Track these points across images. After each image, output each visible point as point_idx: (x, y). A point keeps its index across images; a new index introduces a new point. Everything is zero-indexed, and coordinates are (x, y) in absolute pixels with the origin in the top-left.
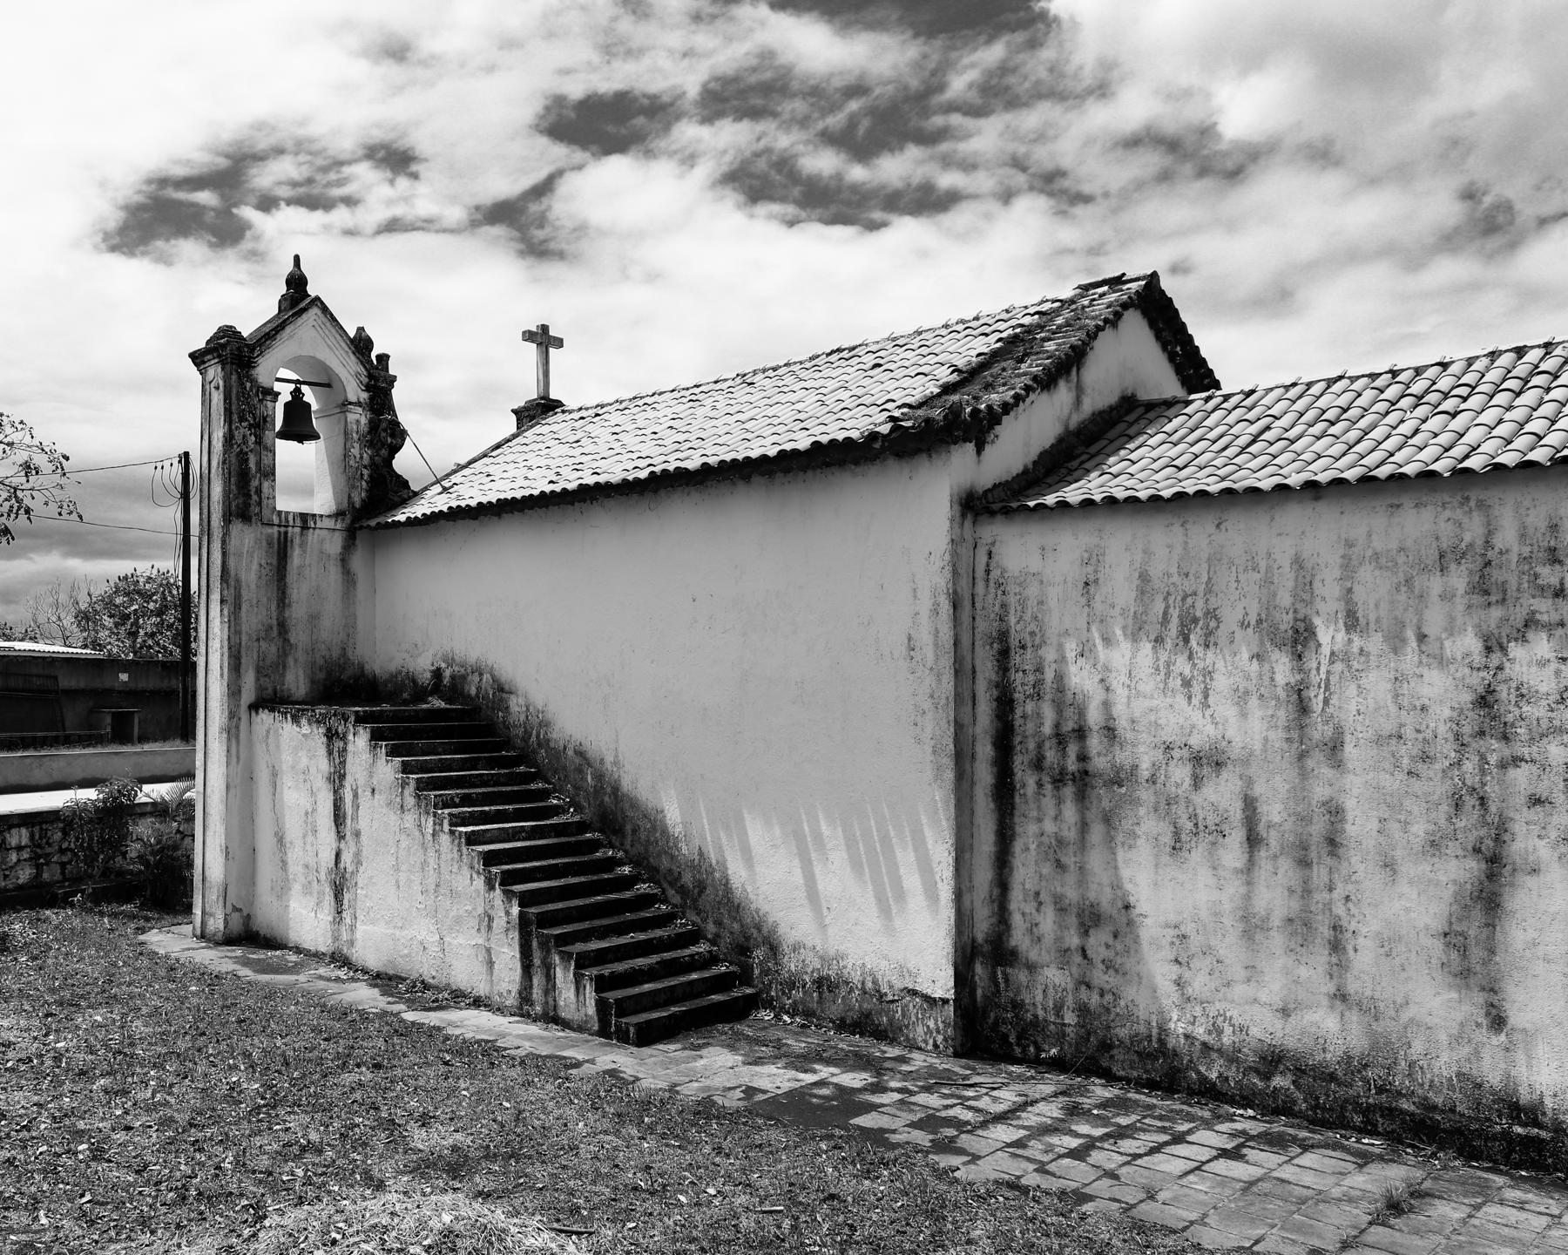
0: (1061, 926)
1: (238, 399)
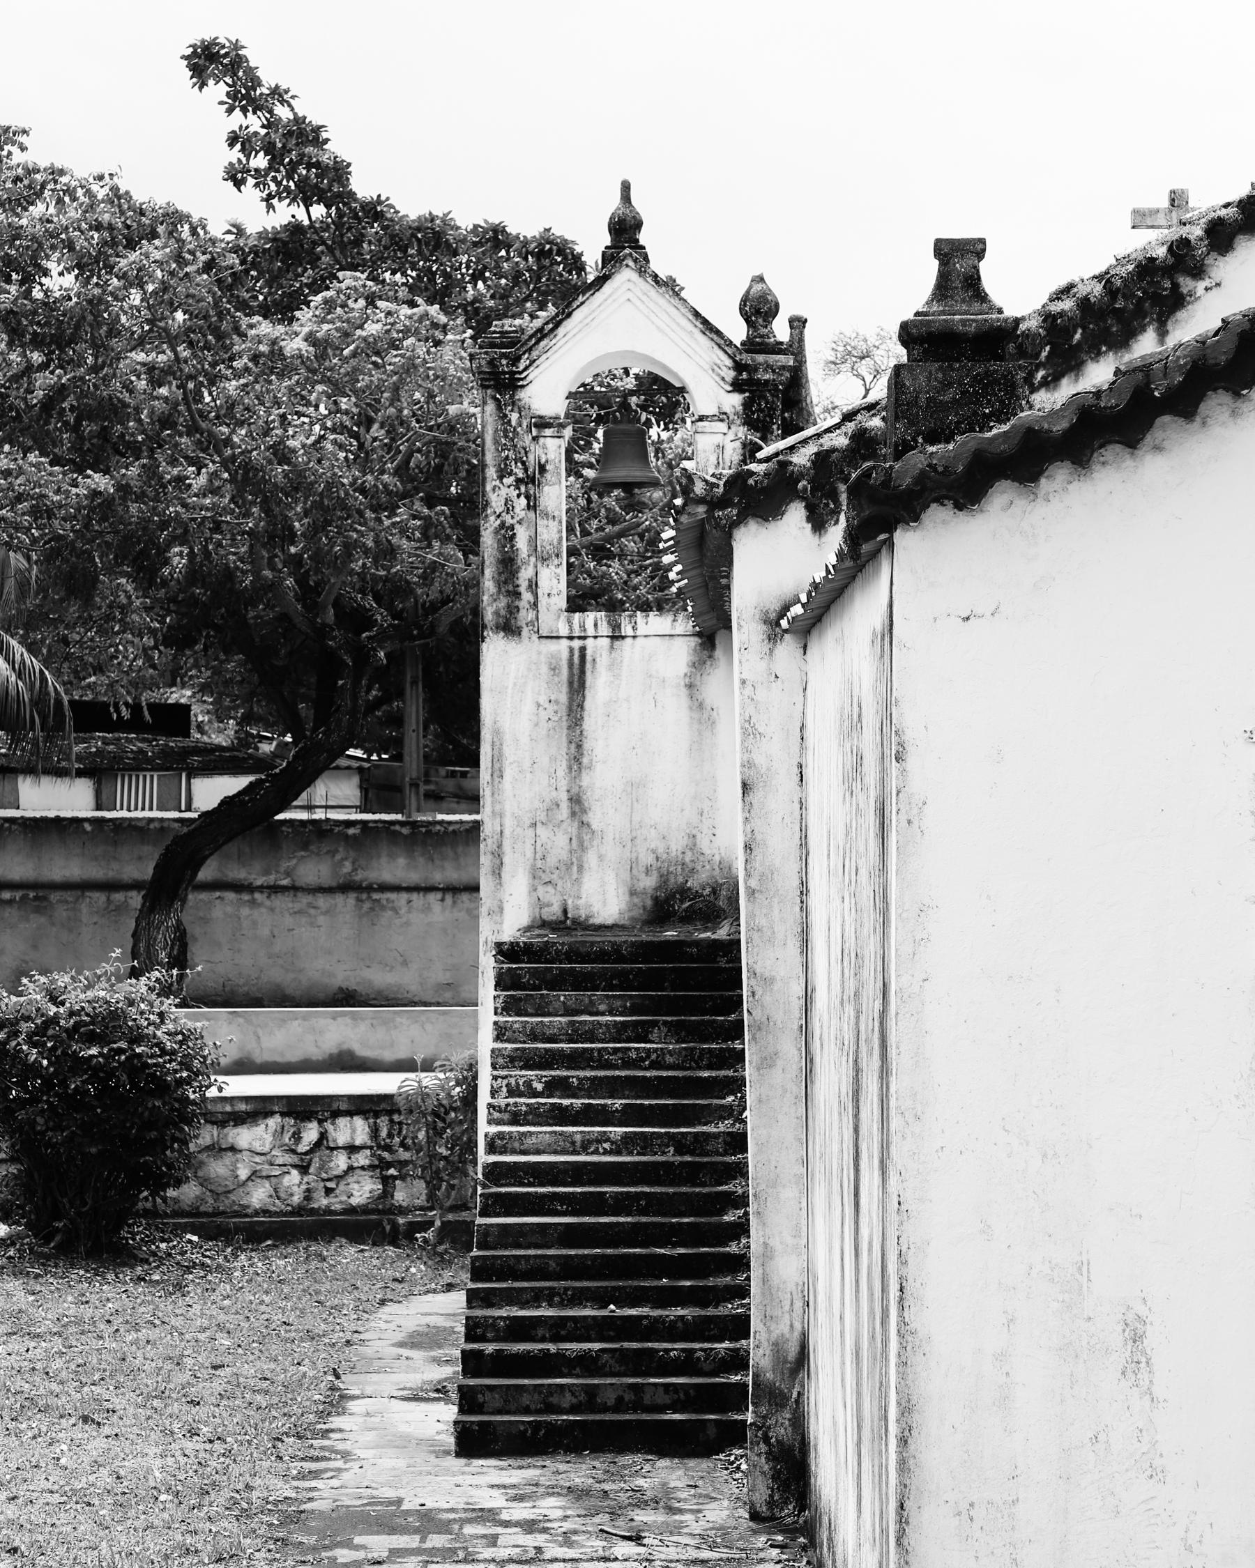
1: (496, 442)
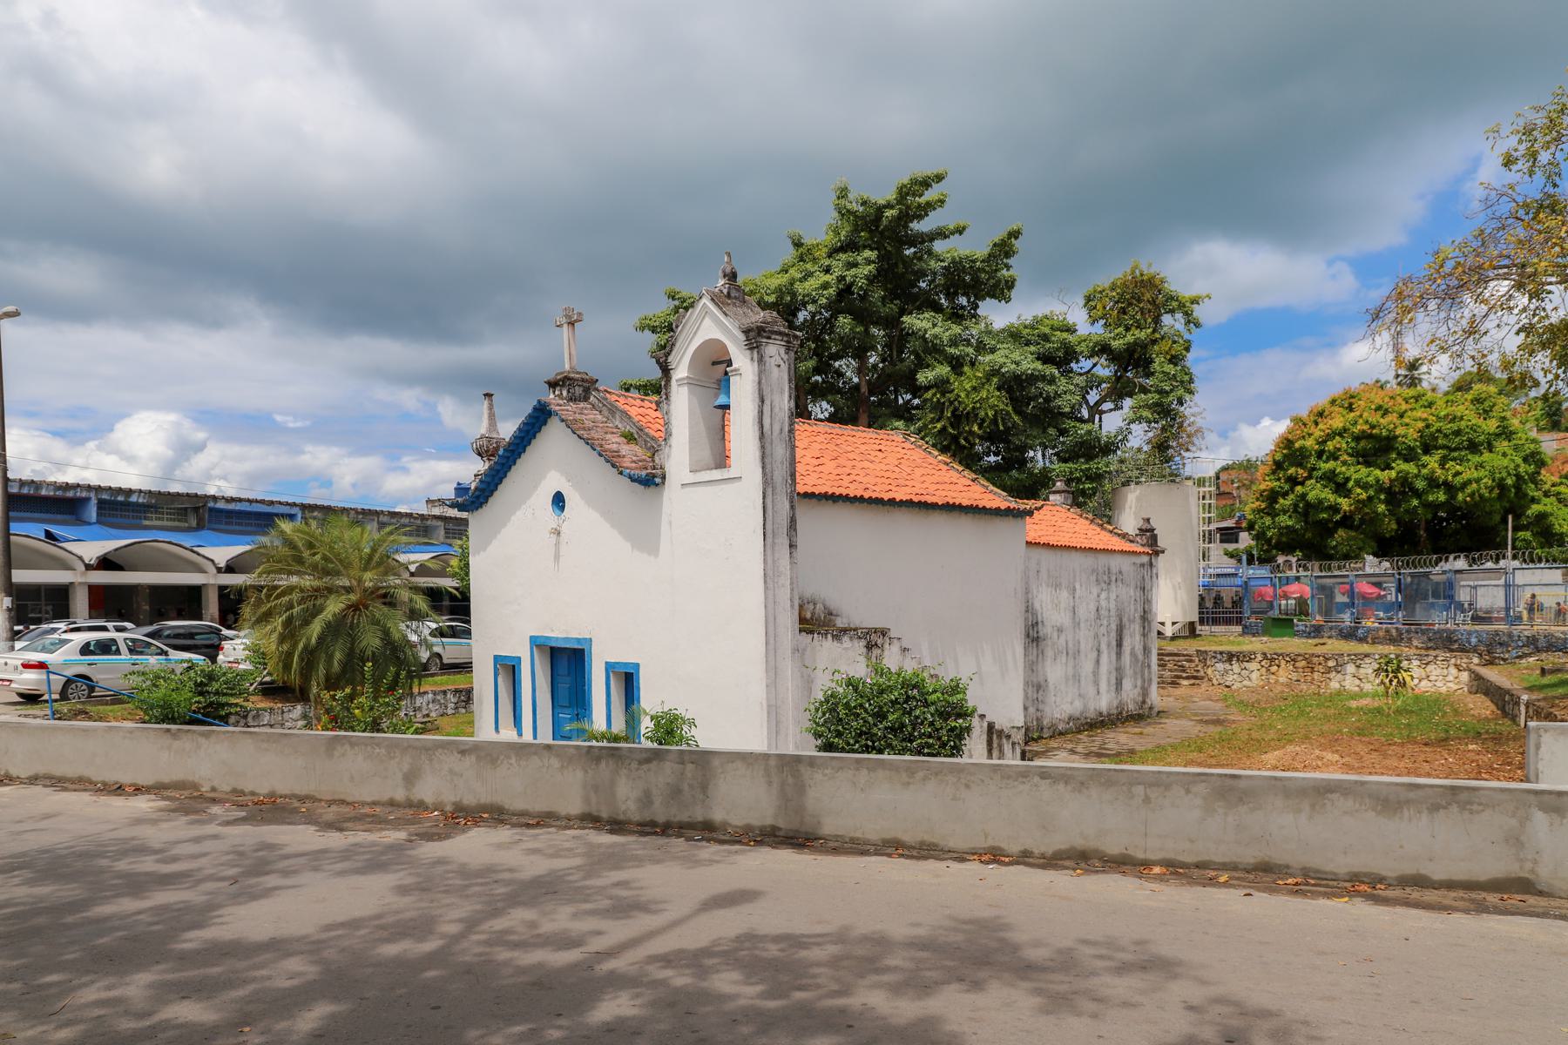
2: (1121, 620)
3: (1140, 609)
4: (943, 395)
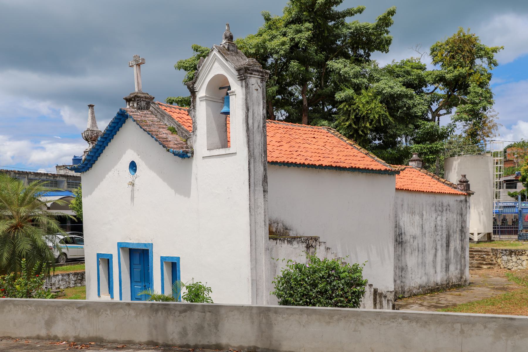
0: (399, 272)
2: (449, 232)
3: (459, 226)
4: (350, 106)
